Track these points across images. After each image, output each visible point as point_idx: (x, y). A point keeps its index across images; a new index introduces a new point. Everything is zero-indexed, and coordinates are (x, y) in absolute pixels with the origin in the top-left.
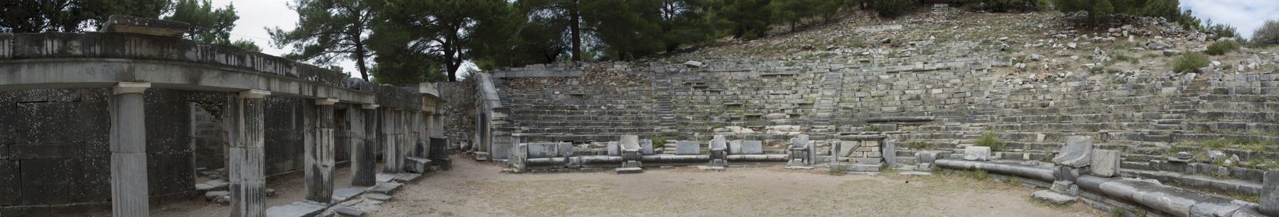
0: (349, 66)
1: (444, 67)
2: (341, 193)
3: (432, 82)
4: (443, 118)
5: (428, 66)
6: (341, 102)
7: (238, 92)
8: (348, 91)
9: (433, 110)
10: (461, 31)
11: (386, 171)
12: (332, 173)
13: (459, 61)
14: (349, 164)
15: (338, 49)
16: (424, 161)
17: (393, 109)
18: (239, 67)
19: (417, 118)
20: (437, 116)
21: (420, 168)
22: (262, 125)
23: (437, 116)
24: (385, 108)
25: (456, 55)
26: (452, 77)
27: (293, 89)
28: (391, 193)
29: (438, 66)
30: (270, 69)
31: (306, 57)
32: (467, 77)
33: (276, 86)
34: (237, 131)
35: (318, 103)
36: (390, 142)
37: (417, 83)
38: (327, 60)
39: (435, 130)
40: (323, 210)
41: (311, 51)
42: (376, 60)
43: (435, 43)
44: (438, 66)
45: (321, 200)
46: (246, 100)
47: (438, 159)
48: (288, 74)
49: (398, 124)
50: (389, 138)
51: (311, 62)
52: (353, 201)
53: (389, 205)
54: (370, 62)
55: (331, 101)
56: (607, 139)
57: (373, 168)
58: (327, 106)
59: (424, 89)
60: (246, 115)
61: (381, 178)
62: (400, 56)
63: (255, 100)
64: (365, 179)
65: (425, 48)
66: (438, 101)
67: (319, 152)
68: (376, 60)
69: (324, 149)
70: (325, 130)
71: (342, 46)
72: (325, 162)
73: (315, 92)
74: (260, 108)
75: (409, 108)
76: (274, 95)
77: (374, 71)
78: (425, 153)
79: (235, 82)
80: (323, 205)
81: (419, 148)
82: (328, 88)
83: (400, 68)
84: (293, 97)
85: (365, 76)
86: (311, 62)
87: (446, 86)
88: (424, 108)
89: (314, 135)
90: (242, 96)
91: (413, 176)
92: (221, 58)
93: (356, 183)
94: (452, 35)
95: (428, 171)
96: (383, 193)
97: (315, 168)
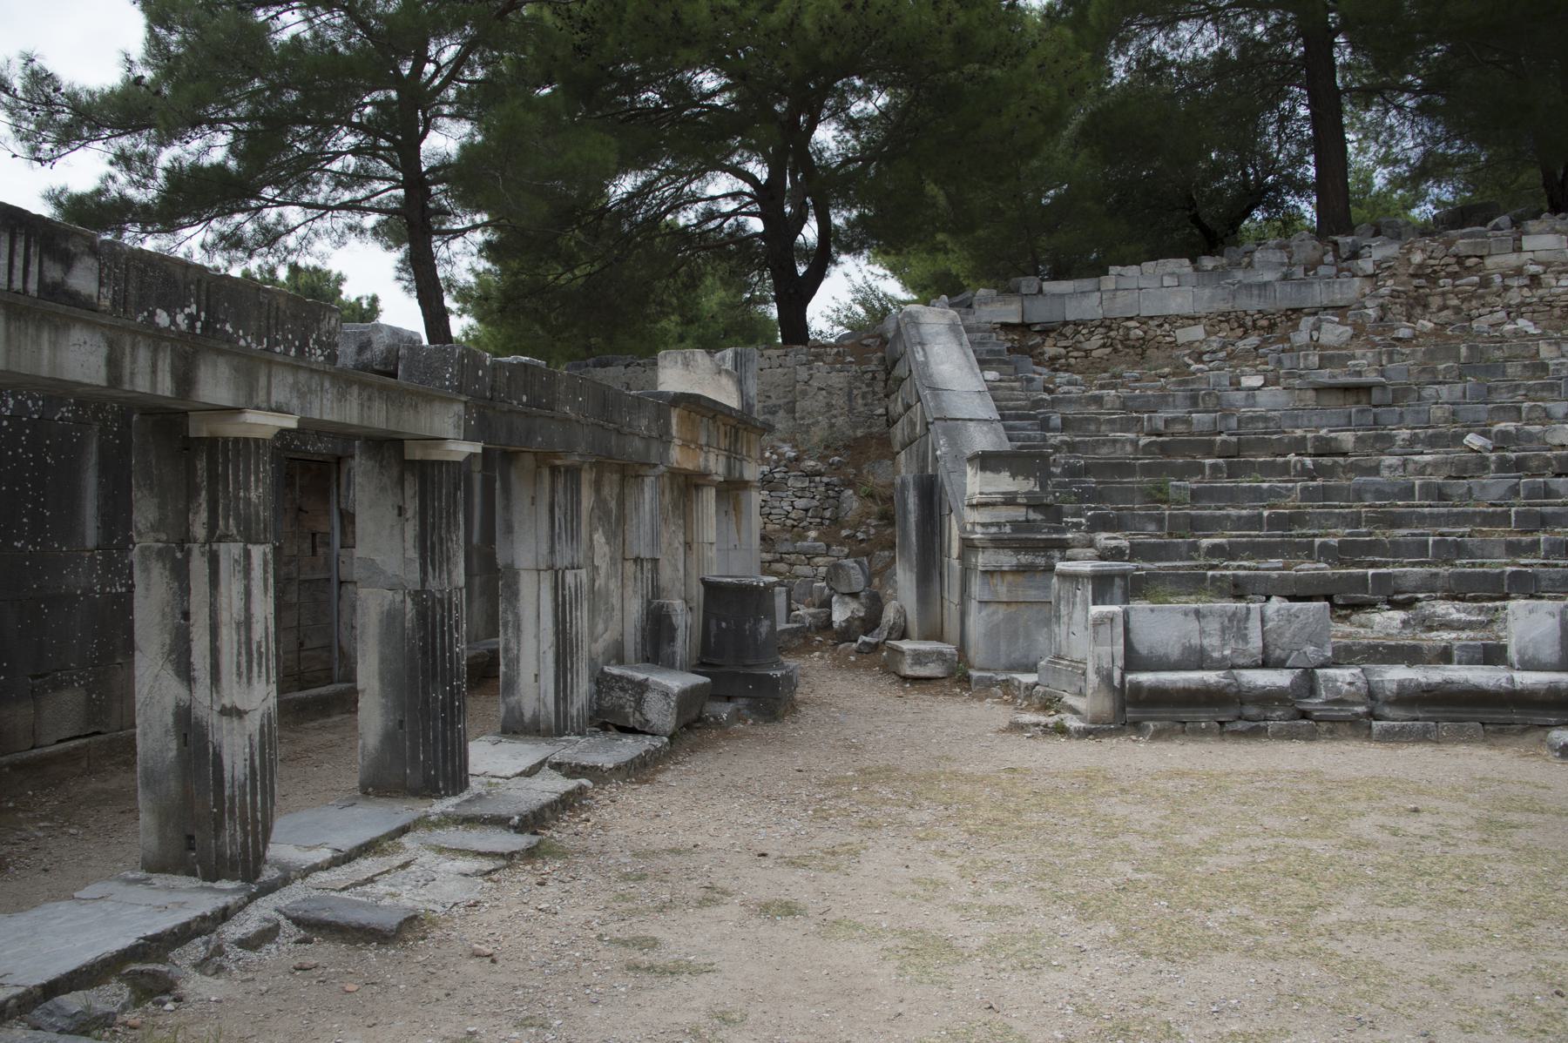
0: (368, 271)
1: (762, 283)
2: (310, 833)
3: (711, 345)
4: (756, 498)
5: (693, 282)
6: (308, 429)
8: (343, 380)
9: (716, 465)
10: (826, 136)
11: (515, 728)
12: (266, 740)
13: (821, 261)
14: (348, 702)
15: (323, 192)
16: (677, 682)
17: (545, 459)
19: (648, 498)
20: (731, 489)
21: (660, 713)
23: (731, 489)
24: (509, 457)
25: (810, 232)
26: (795, 327)
27: (80, 358)
28: (533, 821)
29: (735, 280)
31: (166, 215)
32: (855, 327)
35: (200, 428)
36: (534, 602)
37: (647, 351)
38: (271, 237)
39: (725, 548)
40: (224, 915)
41: (193, 195)
42: (488, 250)
43: (720, 184)
44: (735, 280)
45: (212, 872)
47: (737, 670)
48: (54, 292)
49: (564, 526)
50: (527, 584)
51: (192, 243)
52: (366, 866)
53: (525, 875)
54: (463, 258)
55: (262, 423)
56: (1497, 589)
57: (452, 715)
58: (245, 446)
59: (679, 374)
61: (493, 760)
62: (572, 238)
64: (425, 764)
65: (679, 202)
66: (736, 427)
68: (488, 250)
70: (229, 552)
71: (341, 180)
72: (232, 693)
73: (185, 380)
75: (614, 457)
77: (472, 299)
80: (226, 892)
81: (657, 626)
82: (249, 367)
83: (587, 288)
84: (58, 391)
85: (436, 318)
86: (192, 243)
87: (771, 366)
88: (677, 456)
91: (629, 748)
93: (377, 786)
94: (790, 148)
95: (693, 725)
96: (500, 822)
97: (187, 726)
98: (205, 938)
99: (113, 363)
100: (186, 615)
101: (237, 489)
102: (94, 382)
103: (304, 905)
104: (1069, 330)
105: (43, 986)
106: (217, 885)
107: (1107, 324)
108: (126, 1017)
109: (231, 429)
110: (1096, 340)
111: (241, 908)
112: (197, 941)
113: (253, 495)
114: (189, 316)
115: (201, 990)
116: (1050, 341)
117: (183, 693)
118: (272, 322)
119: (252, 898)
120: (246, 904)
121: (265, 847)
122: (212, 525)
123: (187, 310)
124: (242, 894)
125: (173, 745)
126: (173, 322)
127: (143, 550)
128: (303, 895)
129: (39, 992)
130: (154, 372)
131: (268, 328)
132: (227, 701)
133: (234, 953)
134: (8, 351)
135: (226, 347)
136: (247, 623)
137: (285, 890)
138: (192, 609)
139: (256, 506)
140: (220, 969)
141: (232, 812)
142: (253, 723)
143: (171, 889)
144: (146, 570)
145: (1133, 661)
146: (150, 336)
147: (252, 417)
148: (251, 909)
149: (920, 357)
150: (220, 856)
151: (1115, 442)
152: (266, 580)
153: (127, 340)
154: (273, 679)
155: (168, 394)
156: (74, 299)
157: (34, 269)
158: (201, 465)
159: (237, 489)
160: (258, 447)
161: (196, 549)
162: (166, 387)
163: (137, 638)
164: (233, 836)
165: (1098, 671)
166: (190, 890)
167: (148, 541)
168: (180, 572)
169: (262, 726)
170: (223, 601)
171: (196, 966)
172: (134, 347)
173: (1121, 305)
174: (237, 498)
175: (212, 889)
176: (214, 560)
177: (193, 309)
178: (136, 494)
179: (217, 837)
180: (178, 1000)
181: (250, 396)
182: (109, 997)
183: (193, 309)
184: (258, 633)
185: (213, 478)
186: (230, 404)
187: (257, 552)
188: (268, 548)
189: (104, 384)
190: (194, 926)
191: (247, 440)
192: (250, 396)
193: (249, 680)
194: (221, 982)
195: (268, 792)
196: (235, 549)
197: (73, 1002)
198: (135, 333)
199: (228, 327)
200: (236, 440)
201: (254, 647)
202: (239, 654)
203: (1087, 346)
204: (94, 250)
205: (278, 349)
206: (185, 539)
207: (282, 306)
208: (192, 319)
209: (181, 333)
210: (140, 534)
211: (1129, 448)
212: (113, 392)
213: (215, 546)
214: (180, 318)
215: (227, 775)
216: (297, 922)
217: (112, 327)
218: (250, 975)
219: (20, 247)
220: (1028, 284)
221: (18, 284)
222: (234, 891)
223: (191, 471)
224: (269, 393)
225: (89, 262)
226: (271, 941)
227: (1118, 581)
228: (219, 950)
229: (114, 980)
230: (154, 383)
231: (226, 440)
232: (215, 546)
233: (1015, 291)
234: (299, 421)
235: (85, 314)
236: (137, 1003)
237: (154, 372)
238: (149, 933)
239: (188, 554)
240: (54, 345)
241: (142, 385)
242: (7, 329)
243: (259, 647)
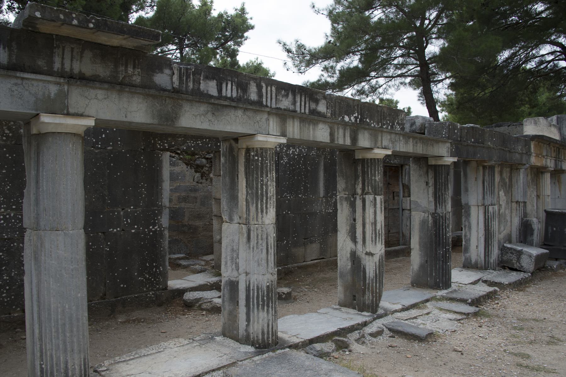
2: (396, 298)
6: (395, 155)
7: (236, 138)
8: (407, 136)
9: (550, 164)
14: (407, 252)
16: (535, 251)
17: (481, 163)
18: (238, 100)
19: (522, 177)
21: (527, 263)
22: (272, 190)
23: (557, 174)
24: (466, 163)
27: (321, 134)
28: (476, 302)
30: (286, 103)
33: (294, 130)
34: (233, 198)
35: (359, 156)
36: (476, 218)
40: (365, 324)
45: (362, 309)
46: (248, 150)
48: (314, 112)
49: (488, 189)
50: (474, 211)
52: (414, 312)
53: (473, 323)
55: (380, 153)
57: (446, 259)
58: (374, 161)
61: (460, 277)
63: (262, 151)
64: (435, 277)
67: (359, 231)
69: (369, 228)
70: (369, 198)
72: (370, 248)
73: (354, 139)
74: (270, 164)
75: (508, 162)
76: (291, 144)
78: (536, 237)
79: (233, 123)
82: (375, 134)
88: (534, 160)
89: (353, 205)
90: (243, 144)
91: (514, 277)
92: (211, 88)
93: (418, 283)
95: (541, 269)
97: (355, 258)
98: (359, 331)
99: (332, 135)
100: (355, 220)
101: (372, 176)
102: (326, 141)
103: (392, 324)
105: (309, 340)
106: (363, 313)
108: (334, 354)
109: (369, 156)
111: (371, 322)
112: (356, 332)
113: (377, 178)
114: (355, 117)
115: (357, 349)
117: (353, 247)
118: (382, 117)
119: (374, 319)
120: (372, 321)
121: (379, 302)
122: (363, 189)
123: (354, 115)
124: (371, 318)
125: (350, 264)
126: (350, 120)
127: (340, 197)
128: (392, 320)
129: (308, 342)
130: (344, 137)
131: (381, 119)
132: (368, 250)
133: (368, 338)
134: (300, 133)
135: (367, 127)
136: (375, 223)
137: (386, 318)
138: (357, 218)
139: (378, 182)
140: (363, 343)
141: (369, 289)
142: (376, 258)
143: (348, 313)
144: (342, 204)
146: (343, 125)
147: (376, 151)
148: (374, 323)
150: (364, 303)
152: (381, 208)
153: (336, 127)
154: (383, 243)
155: (349, 144)
156: (319, 114)
157: (307, 105)
158: (360, 168)
159: (372, 176)
160: (378, 161)
161: (358, 197)
162: (348, 142)
163: (338, 227)
164: (369, 297)
166: (354, 314)
167: (342, 195)
168: (353, 205)
169: (380, 259)
170: (367, 215)
171: (356, 340)
172: (338, 129)
174: (372, 180)
175: (361, 314)
176: (364, 201)
177: (356, 115)
178: (338, 179)
179: (363, 297)
180: (350, 351)
181: (376, 144)
182: (328, 347)
183: (356, 115)
184: (378, 227)
185: (364, 173)
186: (369, 147)
187: (378, 198)
188: (382, 197)
189: (329, 141)
190: (355, 327)
191: (375, 159)
192: (376, 144)
193: (376, 243)
194: (364, 347)
195: (381, 283)
197: (318, 346)
198: (338, 124)
199: (368, 120)
200: (371, 159)
201: (377, 232)
202: (372, 234)
204: (325, 97)
205: (384, 127)
206: (354, 194)
207: (385, 111)
208: (356, 118)
209: (353, 123)
210: (339, 192)
212: (331, 144)
213: (364, 196)
214: (352, 118)
215: (367, 276)
216: (390, 330)
217: (331, 123)
218: (373, 346)
219: (303, 99)
221: (303, 111)
222: (368, 316)
223: (356, 170)
224: (382, 142)
225: (324, 102)
226: (381, 335)
228: (363, 336)
229: (330, 341)
230: (344, 141)
231: (368, 159)
232: (364, 196)
234: (392, 152)
235: (323, 119)
236: (337, 350)
237: (344, 137)
238: (341, 327)
239: (355, 199)
240: (314, 129)
241: (341, 142)
242: (300, 126)
243: (379, 232)
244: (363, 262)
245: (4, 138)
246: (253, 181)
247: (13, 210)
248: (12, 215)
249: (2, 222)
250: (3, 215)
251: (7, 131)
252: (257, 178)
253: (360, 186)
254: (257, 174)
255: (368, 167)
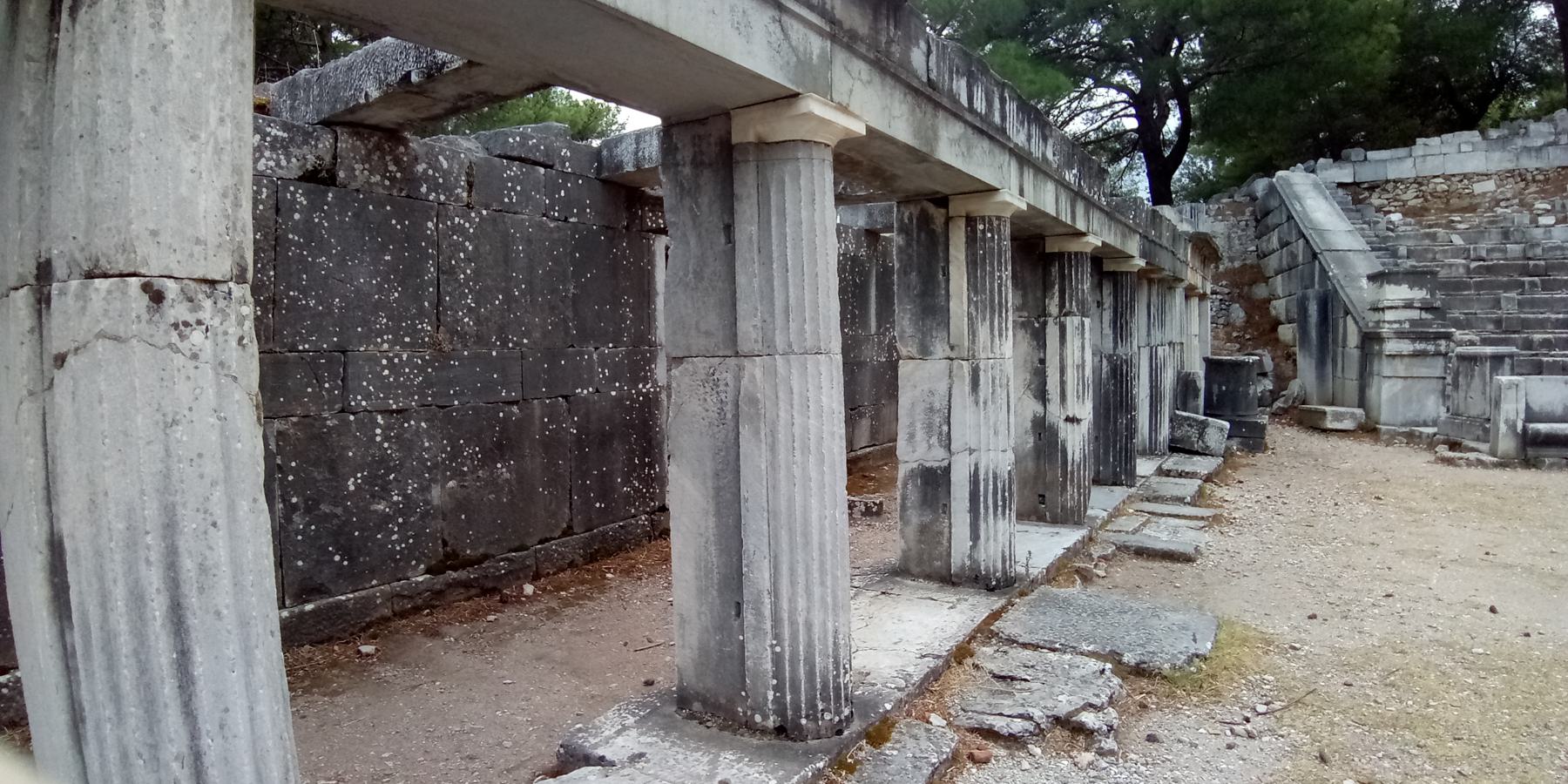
60: (973, 263)
70: (1072, 322)
100: (1043, 361)
104: (1390, 187)
107: (1418, 182)
110: (1411, 194)
116: (1375, 195)
117: (1039, 409)
122: (1062, 305)
145: (1531, 416)
149: (1298, 207)
151: (1451, 266)
161: (1050, 320)
165: (1506, 422)
170: (1069, 351)
173: (1430, 167)
185: (1062, 277)
187: (1087, 321)
196: (1076, 320)
203: (1404, 197)
206: (1044, 313)
211: (1461, 270)
220: (1356, 153)
227: (1507, 360)
231: (1070, 254)
233: (1348, 159)
239: (1045, 324)
244: (1062, 435)
245: (387, 183)
246: (983, 278)
247: (404, 346)
248: (405, 357)
249: (386, 372)
250: (387, 358)
251: (392, 168)
252: (992, 273)
253: (1056, 300)
254: (992, 265)
255: (1070, 267)
